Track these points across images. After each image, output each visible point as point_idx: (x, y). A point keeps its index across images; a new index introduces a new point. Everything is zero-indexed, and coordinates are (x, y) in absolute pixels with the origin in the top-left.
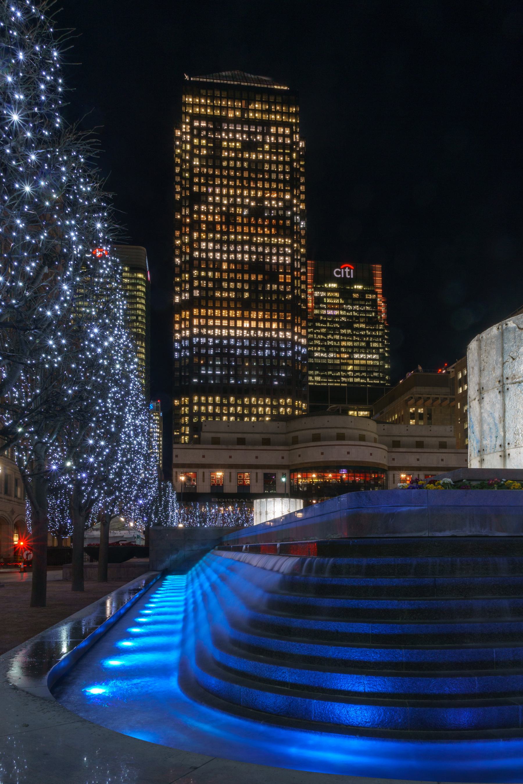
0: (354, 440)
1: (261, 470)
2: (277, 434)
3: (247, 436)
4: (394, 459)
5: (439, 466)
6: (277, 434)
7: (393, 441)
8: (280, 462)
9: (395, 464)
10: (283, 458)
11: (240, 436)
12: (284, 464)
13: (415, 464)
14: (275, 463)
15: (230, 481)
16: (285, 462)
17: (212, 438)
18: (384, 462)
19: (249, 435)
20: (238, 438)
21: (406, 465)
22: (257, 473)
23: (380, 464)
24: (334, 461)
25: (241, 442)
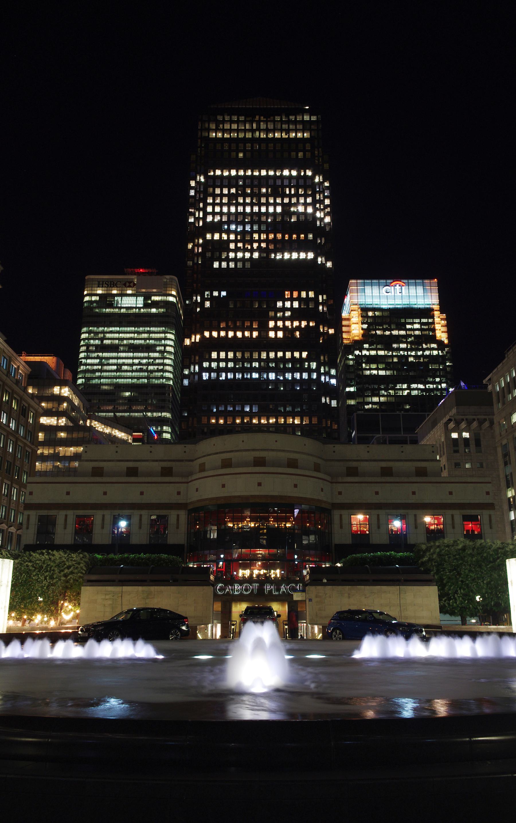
0: (280, 466)
1: (147, 511)
2: (182, 461)
3: (142, 466)
4: (340, 493)
5: (410, 501)
6: (182, 461)
7: (348, 468)
8: (175, 499)
9: (339, 500)
10: (179, 493)
11: (131, 464)
12: (180, 502)
13: (376, 500)
14: (167, 501)
15: (103, 527)
16: (181, 500)
17: (93, 468)
19: (143, 463)
20: (128, 468)
22: (141, 516)
25: (132, 472)
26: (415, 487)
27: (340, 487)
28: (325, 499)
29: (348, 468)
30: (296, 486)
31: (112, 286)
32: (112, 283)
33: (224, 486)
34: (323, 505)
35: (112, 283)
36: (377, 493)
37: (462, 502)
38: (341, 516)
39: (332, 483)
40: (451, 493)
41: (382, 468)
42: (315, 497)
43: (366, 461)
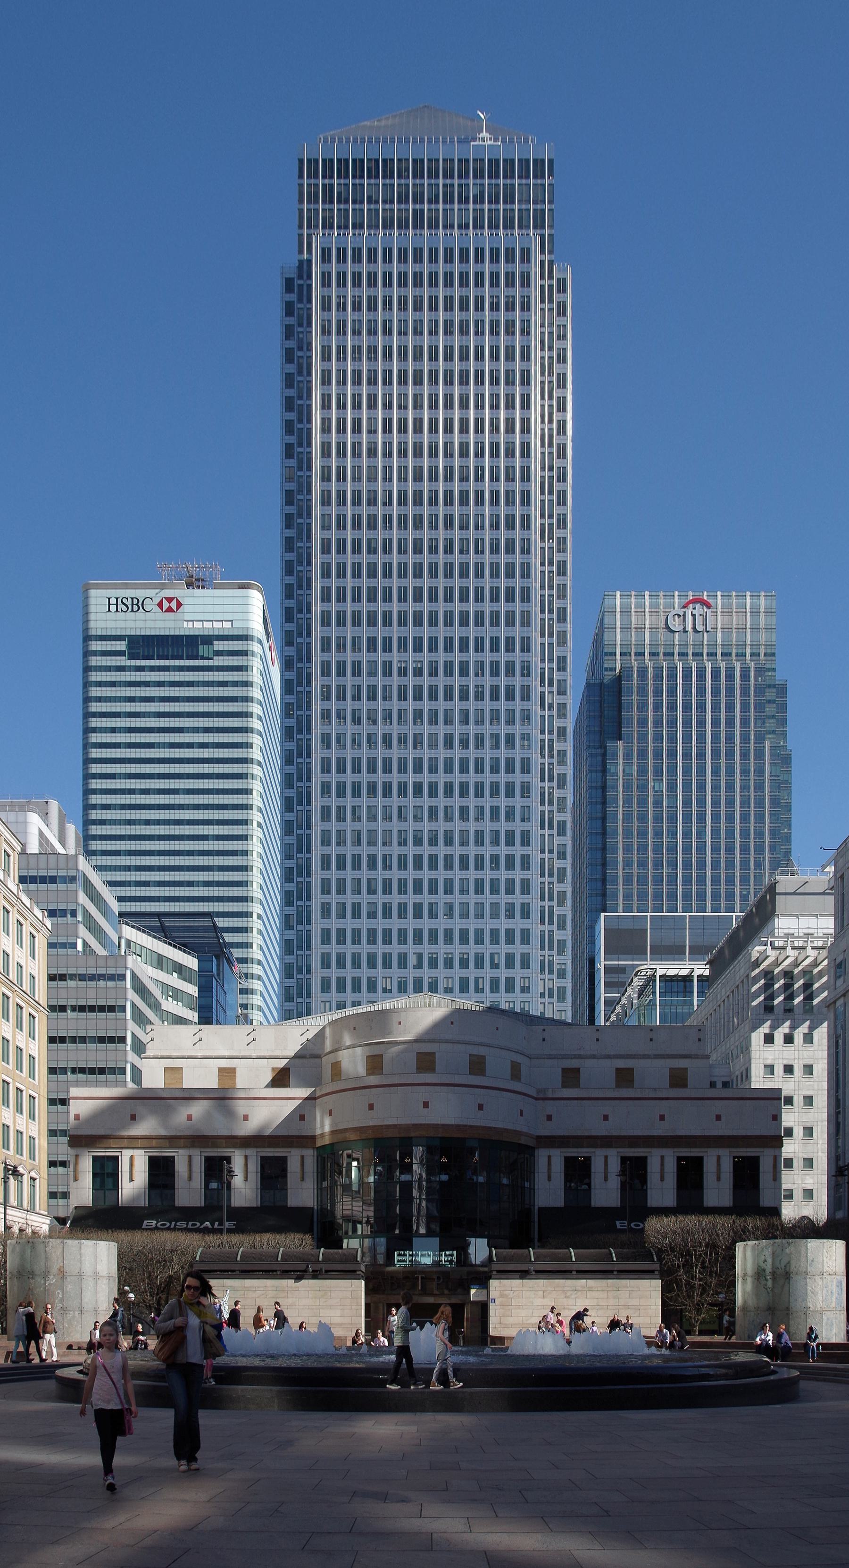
4: (549, 1118)
18: (520, 1125)
21: (579, 1133)
23: (507, 1130)
24: (395, 1126)
26: (663, 1107)
27: (550, 1107)
28: (525, 1129)
29: (565, 1071)
30: (481, 1107)
31: (135, 608)
32: (135, 601)
33: (371, 1107)
34: (523, 1141)
35: (135, 601)
36: (606, 1118)
37: (735, 1133)
38: (549, 1157)
39: (536, 1099)
40: (718, 1118)
41: (617, 1069)
42: (510, 1126)
43: (594, 1057)
